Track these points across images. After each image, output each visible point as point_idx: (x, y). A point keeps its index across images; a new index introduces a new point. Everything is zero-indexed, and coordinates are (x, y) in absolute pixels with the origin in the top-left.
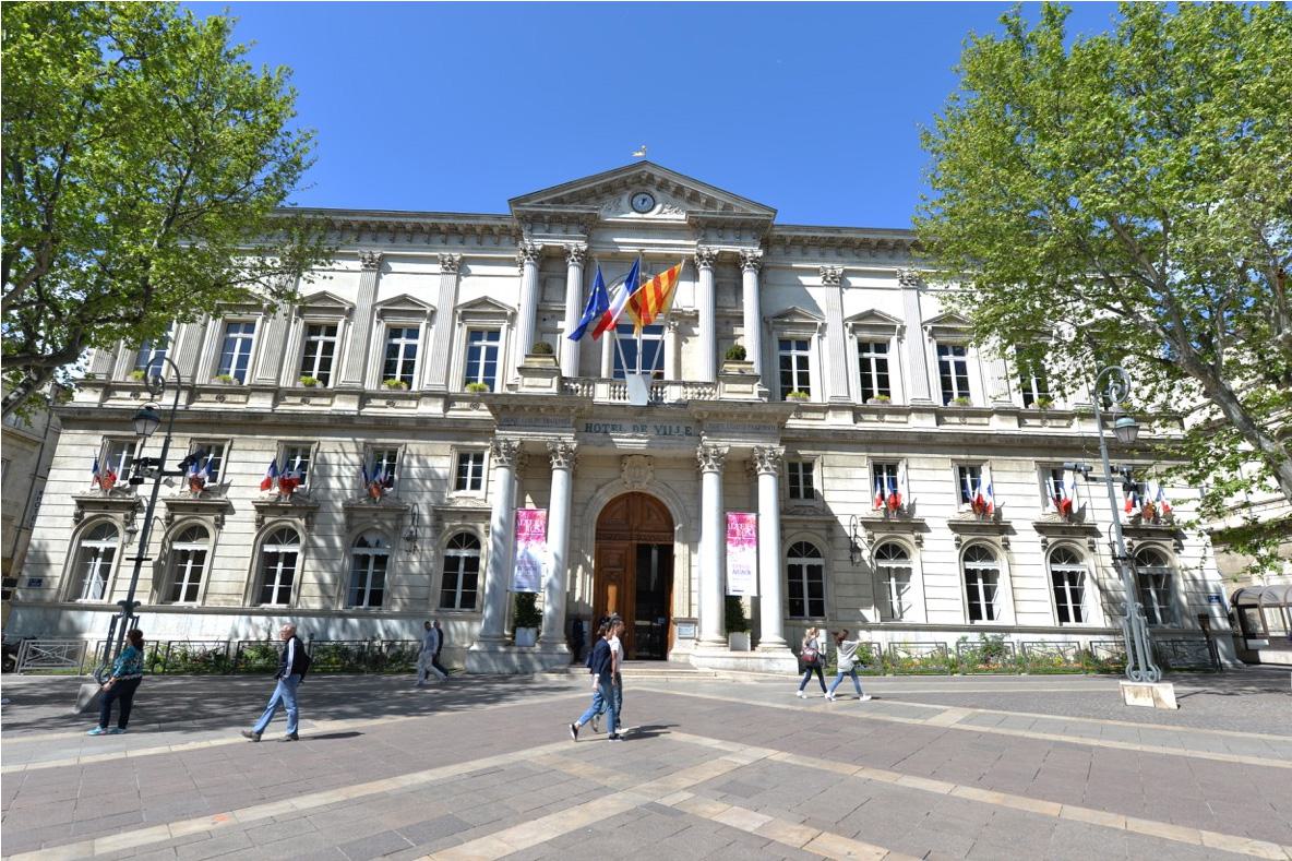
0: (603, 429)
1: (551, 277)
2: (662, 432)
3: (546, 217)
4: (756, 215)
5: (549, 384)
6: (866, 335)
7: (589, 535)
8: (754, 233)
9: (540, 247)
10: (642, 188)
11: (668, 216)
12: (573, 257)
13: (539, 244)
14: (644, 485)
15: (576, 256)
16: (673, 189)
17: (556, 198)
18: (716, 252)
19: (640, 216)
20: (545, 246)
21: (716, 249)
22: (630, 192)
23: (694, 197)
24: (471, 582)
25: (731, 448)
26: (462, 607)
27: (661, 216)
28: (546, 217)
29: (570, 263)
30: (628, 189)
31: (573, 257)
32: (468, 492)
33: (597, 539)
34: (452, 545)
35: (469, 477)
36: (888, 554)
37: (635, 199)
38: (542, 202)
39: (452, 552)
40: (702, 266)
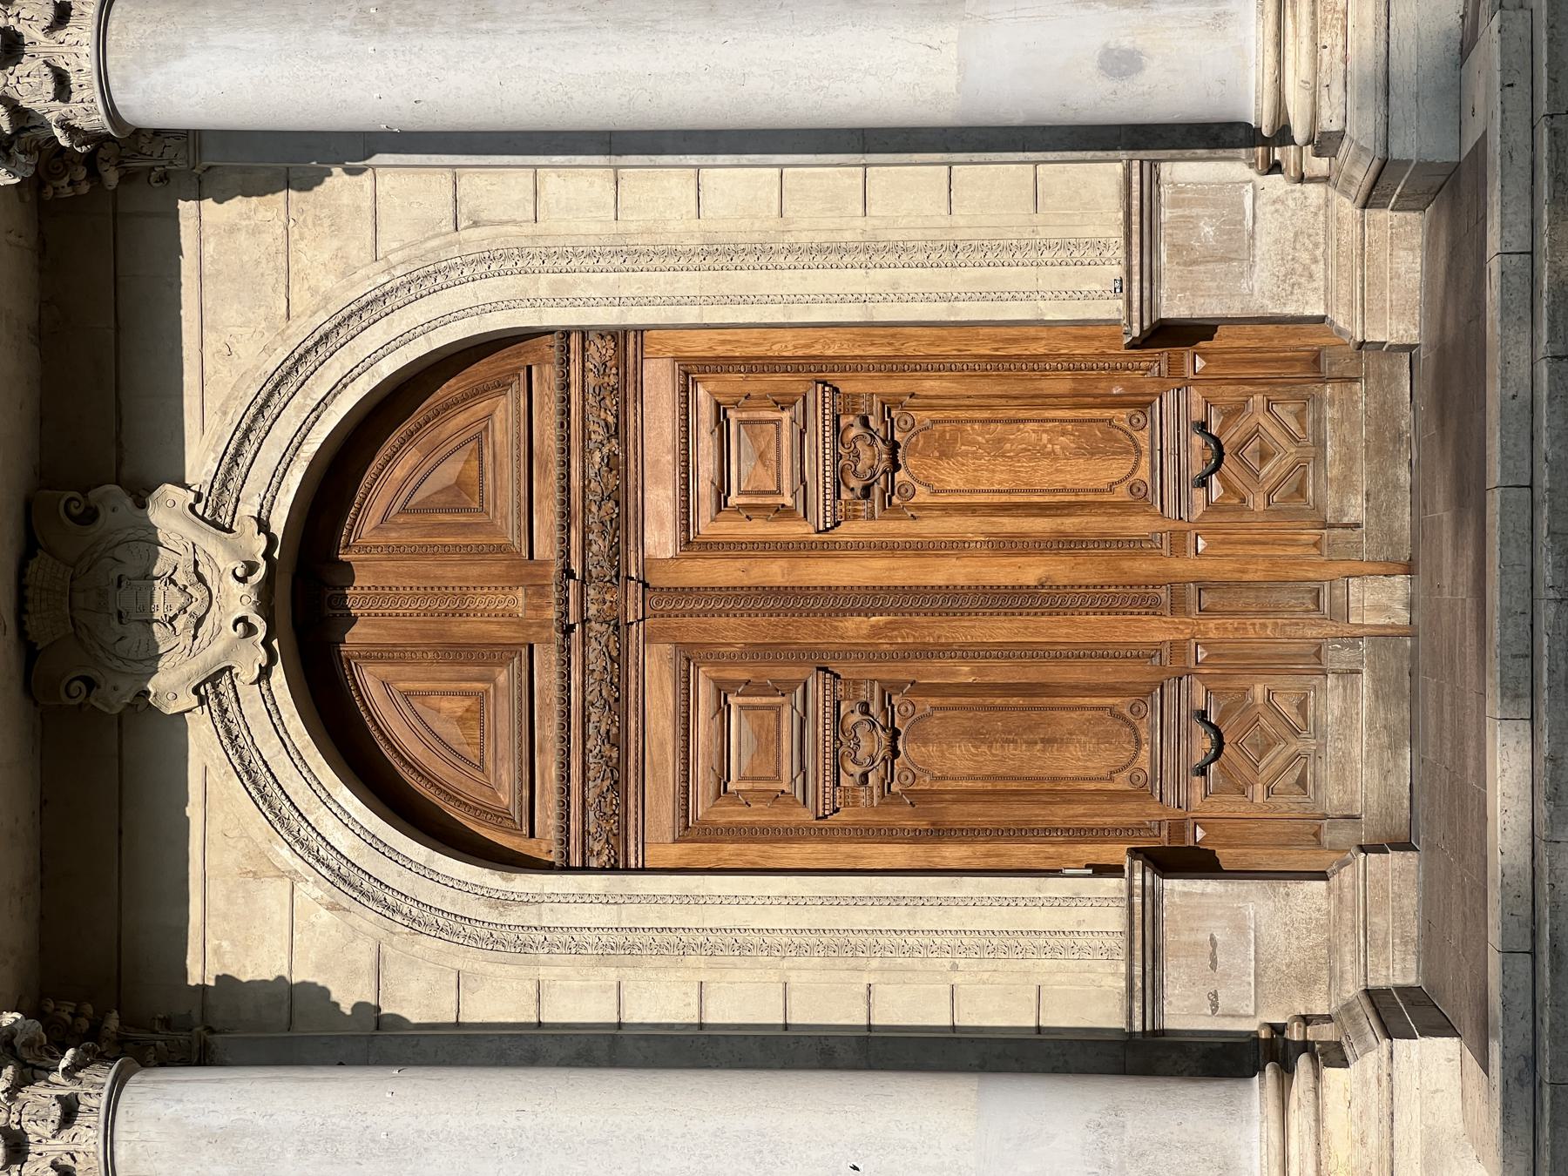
7: (601, 916)
14: (221, 559)
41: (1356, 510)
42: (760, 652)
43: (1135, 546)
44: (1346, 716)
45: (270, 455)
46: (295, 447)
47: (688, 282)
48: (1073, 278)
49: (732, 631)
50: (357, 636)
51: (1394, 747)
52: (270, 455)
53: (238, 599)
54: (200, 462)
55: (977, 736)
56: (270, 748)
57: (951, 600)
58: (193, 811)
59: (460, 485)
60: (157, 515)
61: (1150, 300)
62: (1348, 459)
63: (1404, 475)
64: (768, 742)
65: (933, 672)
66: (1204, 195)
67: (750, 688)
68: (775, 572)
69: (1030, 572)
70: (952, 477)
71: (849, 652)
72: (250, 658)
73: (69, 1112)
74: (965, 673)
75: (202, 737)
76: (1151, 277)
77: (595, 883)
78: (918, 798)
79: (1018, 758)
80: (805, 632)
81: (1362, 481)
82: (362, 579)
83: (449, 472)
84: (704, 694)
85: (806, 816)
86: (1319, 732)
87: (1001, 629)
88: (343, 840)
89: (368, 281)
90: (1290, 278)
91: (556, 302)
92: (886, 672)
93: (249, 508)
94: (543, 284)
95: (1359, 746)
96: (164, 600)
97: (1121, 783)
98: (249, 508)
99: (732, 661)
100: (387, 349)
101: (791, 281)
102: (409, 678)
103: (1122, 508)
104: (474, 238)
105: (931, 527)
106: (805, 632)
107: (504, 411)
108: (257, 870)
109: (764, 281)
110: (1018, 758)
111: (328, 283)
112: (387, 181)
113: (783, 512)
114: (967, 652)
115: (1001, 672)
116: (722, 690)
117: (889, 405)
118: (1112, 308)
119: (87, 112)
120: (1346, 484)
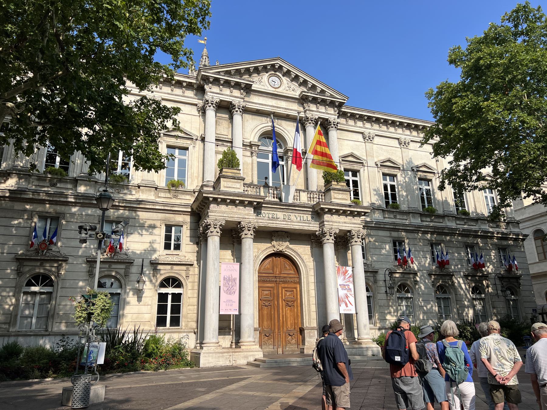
0: (267, 216)
1: (219, 119)
2: (299, 219)
3: (222, 82)
4: (338, 99)
5: (238, 187)
6: (386, 171)
8: (336, 109)
9: (218, 100)
10: (273, 72)
11: (288, 92)
12: (237, 109)
13: (217, 98)
15: (239, 108)
16: (293, 76)
17: (227, 71)
18: (317, 117)
19: (274, 90)
20: (221, 101)
21: (316, 115)
22: (267, 74)
23: (305, 83)
24: (176, 309)
25: (340, 230)
26: (170, 326)
27: (285, 91)
28: (222, 82)
29: (235, 113)
30: (267, 72)
31: (237, 109)
32: (172, 251)
33: (258, 281)
34: (162, 285)
35: (173, 242)
36: (442, 291)
37: (270, 79)
38: (219, 72)
39: (163, 291)
40: (308, 125)
41: (287, 349)
42: (274, 294)
43: (283, 328)
44: (270, 348)
45: (291, 252)
46: (292, 254)
47: (306, 288)
48: (307, 322)
49: (275, 292)
50: (274, 258)
51: (268, 353)
52: (291, 252)
53: (281, 249)
54: (291, 246)
55: (267, 314)
56: (268, 251)
57: (278, 311)
58: (263, 244)
59: (286, 268)
60: (287, 242)
61: (306, 329)
62: (291, 348)
63: (290, 353)
64: (267, 295)
65: (273, 310)
66: (314, 334)
67: (271, 293)
68: (280, 296)
69: (281, 319)
70: (288, 311)
71: (274, 302)
72: (275, 249)
73: (252, 235)
74: (272, 313)
75: (269, 245)
76: (308, 329)
77: (257, 279)
78: (262, 308)
79: (265, 317)
80: (276, 298)
81: (290, 349)
82: (279, 259)
83: (287, 267)
84: (270, 289)
85: (284, 298)
86: (269, 346)
87: (276, 316)
88: (261, 257)
89: (305, 261)
90: (308, 342)
91: (304, 277)
92: (272, 306)
93: (287, 250)
94: (305, 276)
95: (267, 350)
96: (281, 242)
97: (264, 327)
98: (287, 250)
99: (273, 292)
100: (299, 262)
101: (306, 297)
102: (271, 263)
103: (286, 327)
104: (309, 270)
105: (284, 309)
106: (276, 298)
107: (292, 272)
108: (259, 249)
109: (306, 295)
110: (265, 317)
111: (305, 257)
112: (312, 263)
113: (285, 296)
114: (274, 313)
115: (273, 316)
116: (270, 291)
117: (294, 306)
118: (305, 326)
119: (325, 241)
120: (289, 348)
